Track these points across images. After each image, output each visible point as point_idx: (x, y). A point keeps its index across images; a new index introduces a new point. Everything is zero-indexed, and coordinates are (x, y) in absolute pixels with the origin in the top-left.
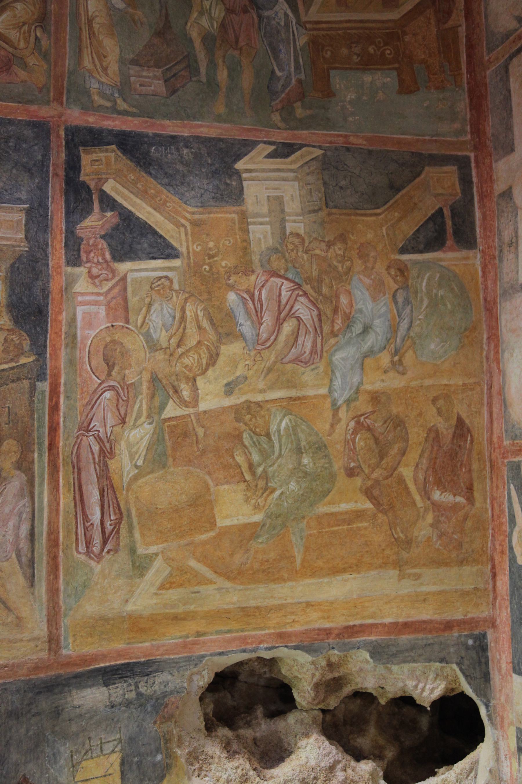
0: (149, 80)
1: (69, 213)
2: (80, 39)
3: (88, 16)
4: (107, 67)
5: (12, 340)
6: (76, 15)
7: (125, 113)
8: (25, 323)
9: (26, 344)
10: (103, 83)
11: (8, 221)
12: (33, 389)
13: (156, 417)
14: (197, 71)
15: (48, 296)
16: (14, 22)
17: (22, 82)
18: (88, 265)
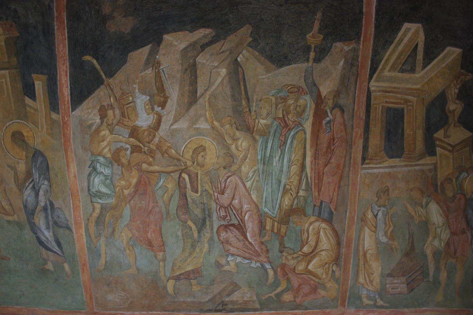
0: (398, 285)
2: (358, 265)
3: (364, 250)
4: (373, 280)
6: (357, 251)
7: (382, 307)
10: (369, 290)
14: (428, 274)
16: (320, 264)
17: (323, 297)
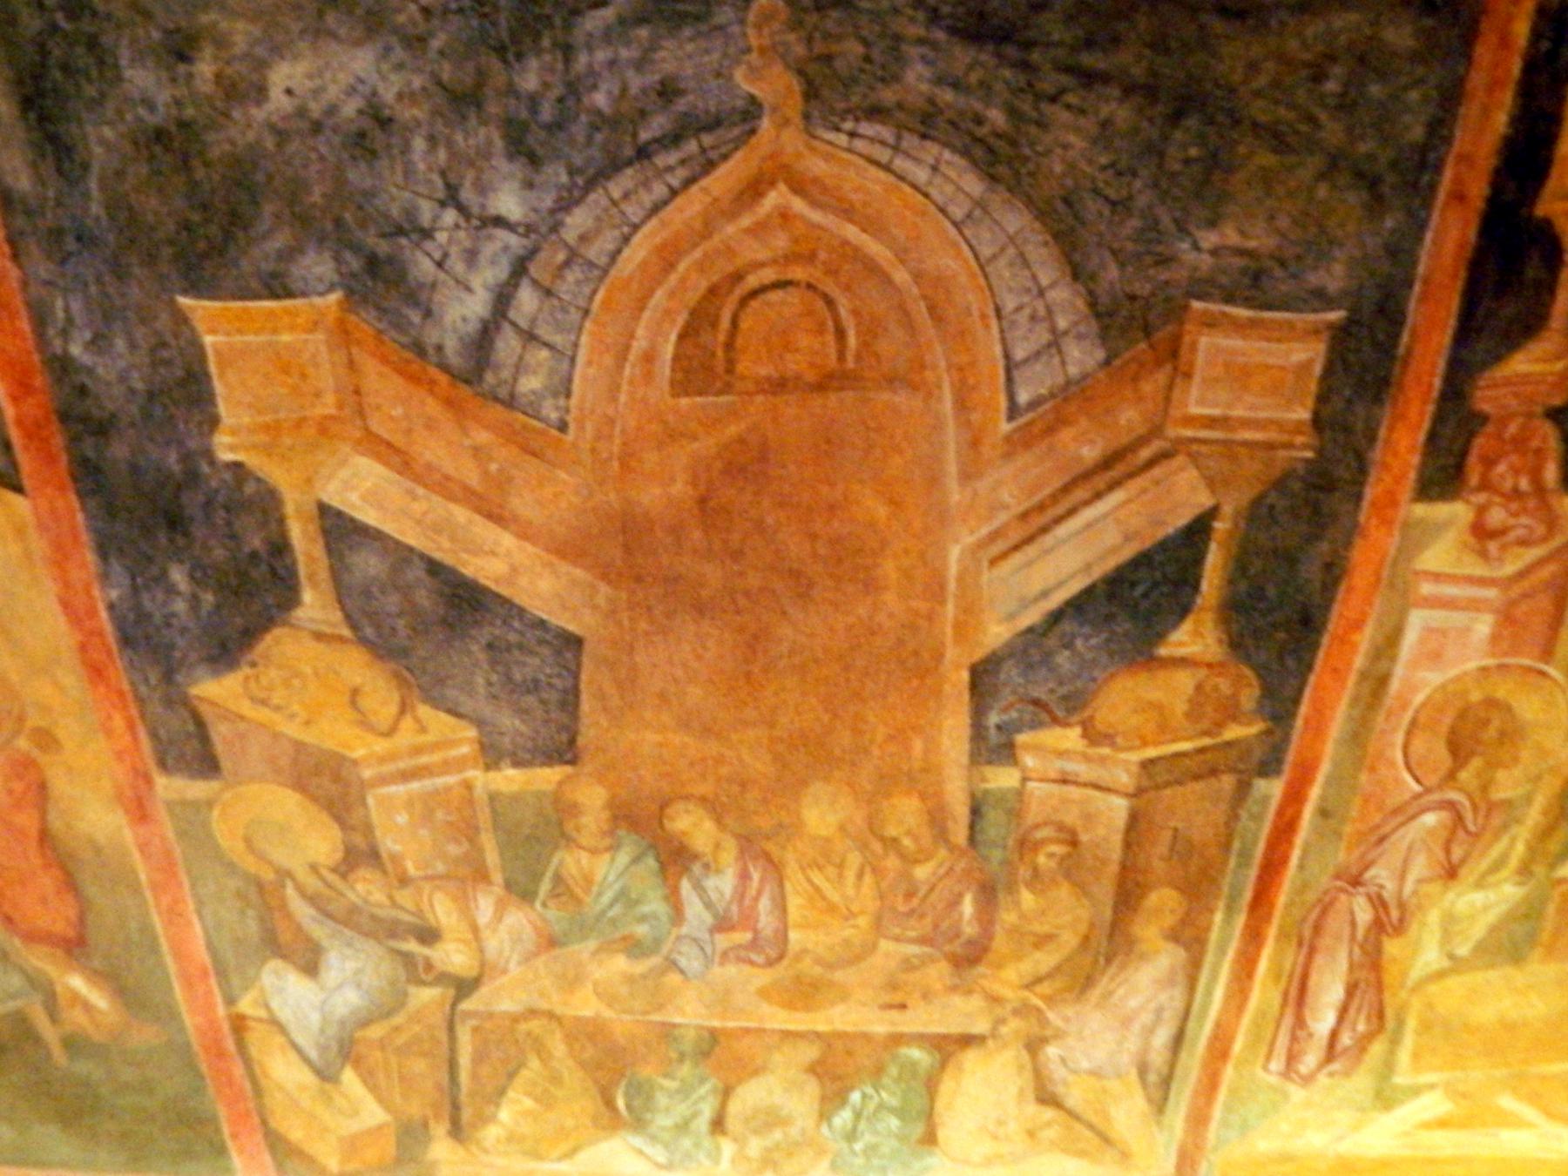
1: (1466, 331)
5: (1216, 688)
8: (1258, 647)
9: (1249, 697)
11: (1268, 367)
12: (1243, 789)
13: (1539, 870)
15: (1336, 581)
18: (1481, 498)
